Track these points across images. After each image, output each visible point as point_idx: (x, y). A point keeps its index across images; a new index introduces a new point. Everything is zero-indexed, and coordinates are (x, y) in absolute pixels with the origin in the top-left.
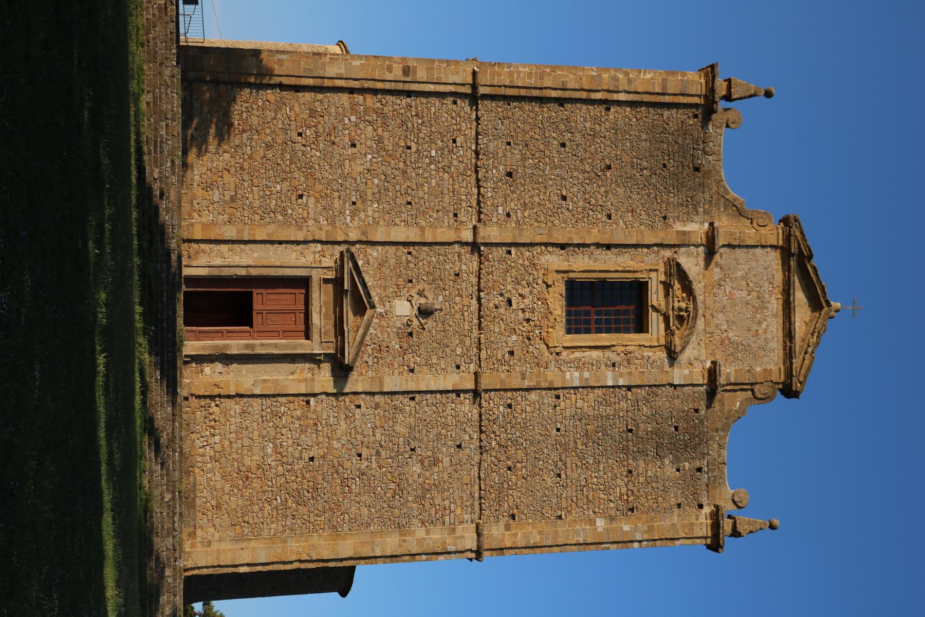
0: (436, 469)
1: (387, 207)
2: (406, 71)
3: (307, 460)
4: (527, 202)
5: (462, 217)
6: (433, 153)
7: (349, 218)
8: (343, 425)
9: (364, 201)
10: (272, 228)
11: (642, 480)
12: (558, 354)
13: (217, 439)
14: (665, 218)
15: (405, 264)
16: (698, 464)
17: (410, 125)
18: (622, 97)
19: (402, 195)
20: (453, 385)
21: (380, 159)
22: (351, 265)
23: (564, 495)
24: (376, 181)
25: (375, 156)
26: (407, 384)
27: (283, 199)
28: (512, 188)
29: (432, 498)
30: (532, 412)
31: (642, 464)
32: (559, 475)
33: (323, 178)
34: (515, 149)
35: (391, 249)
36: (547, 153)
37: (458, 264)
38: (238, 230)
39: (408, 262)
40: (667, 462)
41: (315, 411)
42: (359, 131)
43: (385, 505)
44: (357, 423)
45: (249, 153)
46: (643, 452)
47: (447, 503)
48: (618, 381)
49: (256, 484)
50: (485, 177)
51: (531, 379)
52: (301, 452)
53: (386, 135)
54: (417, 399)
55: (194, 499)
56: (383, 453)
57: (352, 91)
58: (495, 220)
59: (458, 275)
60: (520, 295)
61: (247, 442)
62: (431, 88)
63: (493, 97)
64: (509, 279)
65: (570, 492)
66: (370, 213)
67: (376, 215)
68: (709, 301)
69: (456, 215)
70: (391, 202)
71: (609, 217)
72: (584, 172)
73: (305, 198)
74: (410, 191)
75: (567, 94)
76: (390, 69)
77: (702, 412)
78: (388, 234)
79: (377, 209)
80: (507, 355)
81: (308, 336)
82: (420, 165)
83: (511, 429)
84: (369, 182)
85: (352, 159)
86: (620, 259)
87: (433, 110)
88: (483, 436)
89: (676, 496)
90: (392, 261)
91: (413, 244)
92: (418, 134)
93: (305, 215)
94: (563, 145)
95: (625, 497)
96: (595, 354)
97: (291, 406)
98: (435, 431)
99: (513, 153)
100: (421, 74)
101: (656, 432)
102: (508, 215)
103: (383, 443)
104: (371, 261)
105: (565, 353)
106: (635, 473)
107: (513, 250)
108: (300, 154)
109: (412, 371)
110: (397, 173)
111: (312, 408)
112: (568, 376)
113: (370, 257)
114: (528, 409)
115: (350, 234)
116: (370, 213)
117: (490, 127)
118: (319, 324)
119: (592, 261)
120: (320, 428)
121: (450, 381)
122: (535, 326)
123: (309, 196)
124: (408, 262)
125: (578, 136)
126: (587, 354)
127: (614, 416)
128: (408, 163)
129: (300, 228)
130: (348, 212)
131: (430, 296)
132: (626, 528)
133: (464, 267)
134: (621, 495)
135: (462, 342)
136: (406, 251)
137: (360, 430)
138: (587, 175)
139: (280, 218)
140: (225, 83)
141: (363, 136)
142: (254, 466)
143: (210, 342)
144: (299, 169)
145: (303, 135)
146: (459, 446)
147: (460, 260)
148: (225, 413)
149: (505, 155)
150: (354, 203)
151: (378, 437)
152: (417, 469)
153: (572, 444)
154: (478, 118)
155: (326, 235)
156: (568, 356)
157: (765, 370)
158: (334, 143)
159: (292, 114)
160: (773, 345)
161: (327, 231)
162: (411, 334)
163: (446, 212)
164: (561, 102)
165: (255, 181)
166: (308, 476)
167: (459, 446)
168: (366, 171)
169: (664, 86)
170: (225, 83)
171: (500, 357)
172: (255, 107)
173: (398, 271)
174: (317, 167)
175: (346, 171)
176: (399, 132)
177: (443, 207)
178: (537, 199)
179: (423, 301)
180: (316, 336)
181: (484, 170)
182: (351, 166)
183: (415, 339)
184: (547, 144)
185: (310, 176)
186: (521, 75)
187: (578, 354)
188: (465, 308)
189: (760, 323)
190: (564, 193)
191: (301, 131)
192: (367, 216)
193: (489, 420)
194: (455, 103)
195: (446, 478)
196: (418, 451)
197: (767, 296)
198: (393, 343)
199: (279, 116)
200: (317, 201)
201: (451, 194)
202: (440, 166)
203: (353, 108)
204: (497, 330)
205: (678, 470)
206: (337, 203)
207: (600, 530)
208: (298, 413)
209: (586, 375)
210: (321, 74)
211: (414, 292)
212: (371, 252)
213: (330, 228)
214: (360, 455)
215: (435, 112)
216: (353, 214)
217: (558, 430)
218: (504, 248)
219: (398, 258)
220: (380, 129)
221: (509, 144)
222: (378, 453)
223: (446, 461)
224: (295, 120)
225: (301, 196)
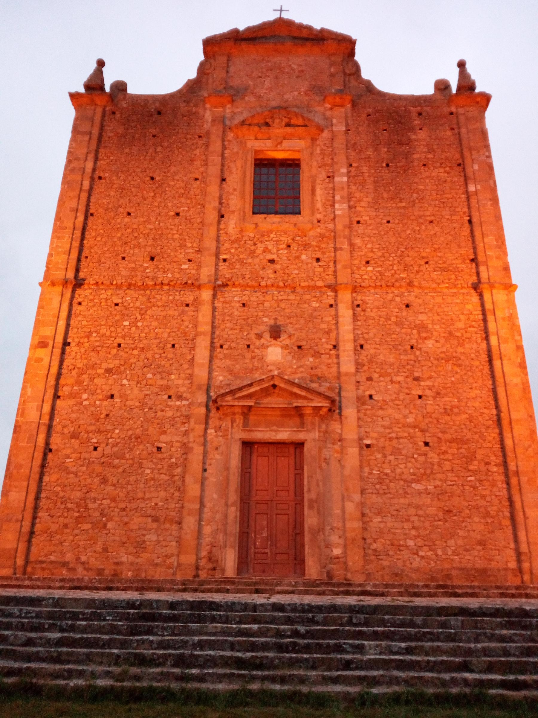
0: (430, 326)
1: (176, 365)
2: (43, 345)
3: (427, 448)
4: (178, 244)
6: (126, 323)
7: (185, 402)
8: (390, 411)
9: (168, 387)
10: (189, 480)
11: (430, 156)
12: (319, 222)
13: (411, 543)
14: (200, 137)
15: (231, 351)
16: (414, 114)
17: (97, 344)
18: (89, 165)
19: (164, 352)
20: (349, 309)
21: (128, 372)
22: (229, 398)
23: (449, 217)
24: (149, 376)
25: (124, 376)
26: (348, 351)
27: (160, 466)
28: (165, 256)
29: (458, 330)
30: (373, 243)
31: (417, 156)
32: (431, 222)
33: (142, 426)
34: (128, 253)
35: (217, 363)
36: (135, 226)
37: (233, 304)
38: (190, 514)
39: (230, 348)
40: (414, 137)
41: (377, 439)
42: (98, 391)
43: (469, 373)
44: (388, 398)
45: (108, 501)
46: (407, 155)
47: (462, 317)
48: (343, 173)
49: (456, 501)
50: (153, 279)
52: (420, 455)
53: (105, 366)
54: (362, 342)
55: (477, 570)
56: (416, 374)
57: (56, 397)
58: (193, 272)
59: (244, 305)
60: (264, 252)
61: (412, 511)
62: (62, 324)
63: (77, 270)
64: (250, 261)
66: (180, 382)
67: (182, 376)
69: (187, 305)
70: (171, 362)
73: (160, 445)
74: (161, 345)
75: (82, 208)
76: (39, 360)
77: (370, 111)
79: (177, 375)
80: (320, 263)
81: (299, 445)
82: (137, 335)
83: (389, 261)
84: (150, 382)
85: (124, 397)
86: (234, 170)
87: (84, 323)
88: (397, 284)
90: (228, 362)
91: (212, 343)
92: (106, 336)
93: (179, 444)
95: (448, 169)
97: (373, 463)
98: (394, 327)
99: (133, 255)
100: (48, 331)
101: (388, 144)
102: (190, 261)
103: (406, 374)
104: (227, 382)
105: (319, 216)
107: (223, 257)
108: (115, 449)
110: (143, 356)
111: (375, 442)
113: (223, 383)
114: (369, 246)
115: (199, 401)
116: (180, 382)
117: (106, 273)
118: (288, 433)
119: (235, 193)
120: (393, 435)
122: (293, 239)
123: (159, 441)
124: (230, 348)
125: (122, 201)
126: (318, 197)
127: (375, 177)
128: (133, 346)
129: (191, 449)
130: (178, 403)
131: (262, 328)
133: (236, 299)
134: (445, 172)
135: (308, 302)
136: (219, 350)
137: (395, 396)
138: (157, 195)
139: (179, 470)
140: (33, 524)
141: (103, 387)
142: (436, 503)
143: (306, 547)
144: (131, 449)
145: (96, 445)
146: (407, 306)
147: (230, 302)
148: (381, 532)
149: (134, 262)
150: (170, 397)
151: (400, 379)
152: (430, 343)
155: (200, 424)
156: (320, 213)
158: (107, 415)
159: (74, 455)
160: (311, 60)
161: (195, 423)
162: (299, 347)
163: (183, 313)
164: (88, 214)
165: (140, 495)
166: (444, 448)
168: (139, 385)
169: (85, 133)
170: (33, 524)
171: (321, 270)
172: (61, 494)
173: (237, 357)
174: (130, 432)
175: (137, 404)
176: (103, 353)
177: (179, 315)
179: (267, 335)
180: (301, 436)
181: (146, 279)
182: (132, 399)
183: (304, 343)
184: (127, 227)
186: (60, 245)
187: (319, 205)
188: (275, 298)
189: (293, 69)
190: (173, 213)
191: (92, 448)
192: (183, 385)
193: (382, 279)
195: (439, 318)
196: (413, 342)
197: (270, 64)
198: (308, 363)
199: (74, 469)
200: (164, 433)
201: (167, 308)
202: (139, 317)
203: (73, 395)
204: (296, 272)
205: (421, 129)
206: (169, 414)
207: (479, 187)
210: (34, 426)
211: (257, 342)
212: (219, 382)
213: (192, 421)
214: (420, 397)
215: (87, 321)
216: (180, 397)
217: (388, 222)
218: (220, 264)
219: (226, 357)
220: (99, 371)
221: (123, 258)
222: (416, 379)
223: (422, 317)
224: (80, 453)
225: (159, 449)
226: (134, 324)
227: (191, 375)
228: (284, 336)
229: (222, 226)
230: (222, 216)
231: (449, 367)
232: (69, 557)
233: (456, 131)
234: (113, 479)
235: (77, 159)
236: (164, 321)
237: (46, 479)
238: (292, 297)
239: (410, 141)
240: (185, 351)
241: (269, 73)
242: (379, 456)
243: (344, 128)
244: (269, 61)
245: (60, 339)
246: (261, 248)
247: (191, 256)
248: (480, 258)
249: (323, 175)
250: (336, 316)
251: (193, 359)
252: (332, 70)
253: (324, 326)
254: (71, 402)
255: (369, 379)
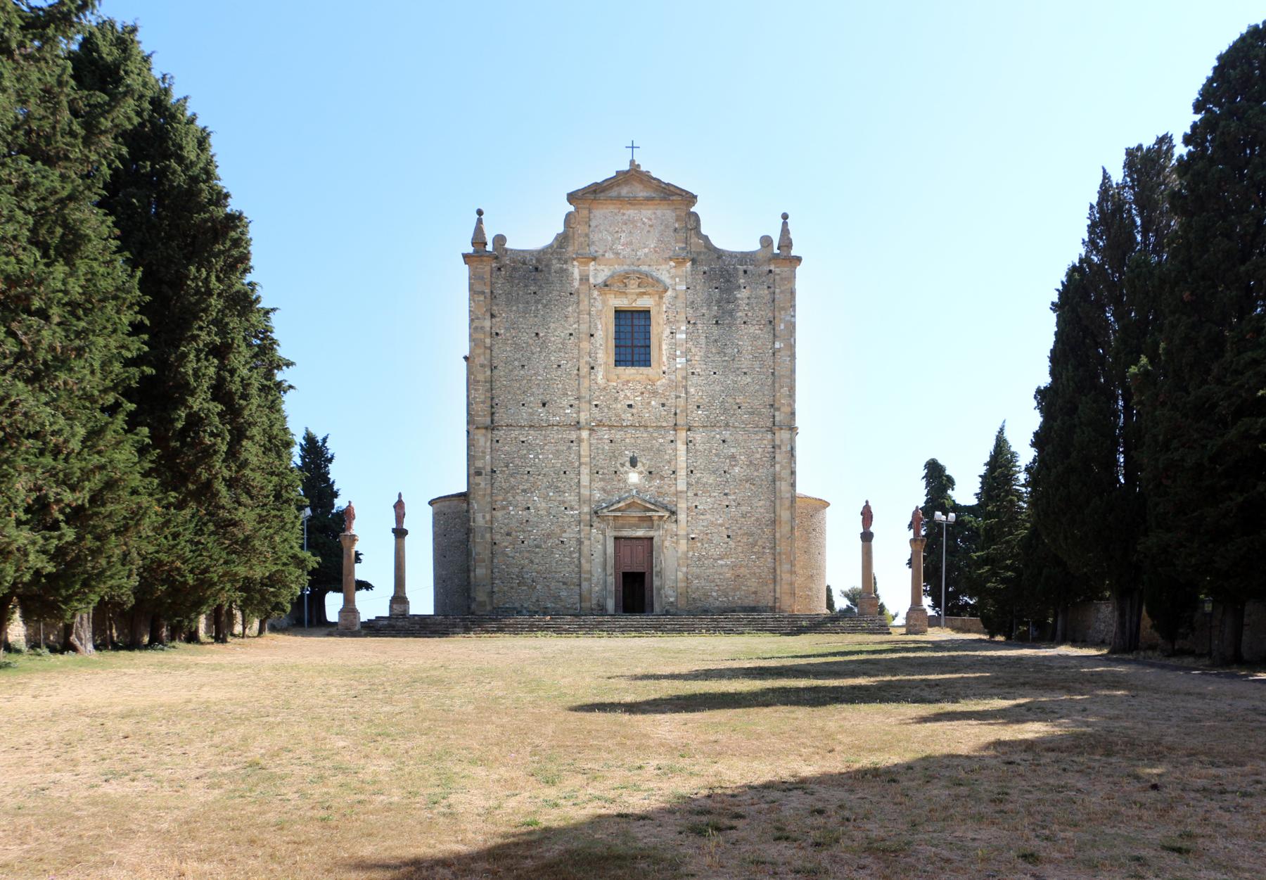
5: (573, 436)
8: (708, 516)
9: (564, 502)
10: (583, 561)
13: (714, 594)
16: (741, 273)
24: (551, 494)
29: (756, 459)
31: (740, 314)
32: (745, 373)
40: (739, 296)
44: (707, 508)
46: (731, 313)
49: (742, 570)
51: (681, 392)
65: (757, 364)
68: (628, 261)
71: (571, 334)
72: (540, 352)
77: (706, 268)
78: (585, 486)
85: (537, 509)
86: (600, 327)
89: (763, 289)
94: (523, 366)
96: (664, 347)
101: (718, 302)
105: (664, 368)
106: (745, 319)
109: (674, 472)
112: (679, 366)
116: (572, 498)
121: (681, 448)
124: (603, 474)
126: (664, 352)
132: (782, 326)
134: (760, 329)
144: (545, 542)
146: (724, 441)
147: (601, 439)
152: (737, 469)
153: (725, 364)
154: (507, 426)
157: (677, 220)
160: (659, 212)
162: (650, 473)
163: (569, 448)
167: (724, 441)
178: (560, 386)
179: (628, 464)
180: (651, 534)
184: (523, 378)
185: (549, 536)
187: (664, 359)
189: (644, 223)
194: (498, 441)
196: (726, 468)
203: (504, 508)
206: (567, 520)
208: (699, 544)
209: (678, 353)
216: (572, 509)
219: (601, 480)
222: (726, 494)
223: (733, 450)
225: (562, 542)
226: (536, 456)
227: (579, 493)
228: (639, 464)
229: (592, 377)
230: (593, 368)
231: (747, 485)
232: (517, 605)
233: (772, 290)
234: (537, 561)
235: (478, 318)
236: (557, 454)
237: (495, 561)
238: (645, 435)
239: (736, 299)
240: (573, 476)
241: (624, 228)
242: (699, 544)
243: (684, 288)
244: (624, 214)
245: (488, 469)
246: (622, 395)
247: (572, 402)
248: (776, 405)
249: (668, 331)
250: (676, 450)
251: (579, 482)
252: (677, 226)
253: (667, 457)
254: (505, 512)
255: (696, 495)
